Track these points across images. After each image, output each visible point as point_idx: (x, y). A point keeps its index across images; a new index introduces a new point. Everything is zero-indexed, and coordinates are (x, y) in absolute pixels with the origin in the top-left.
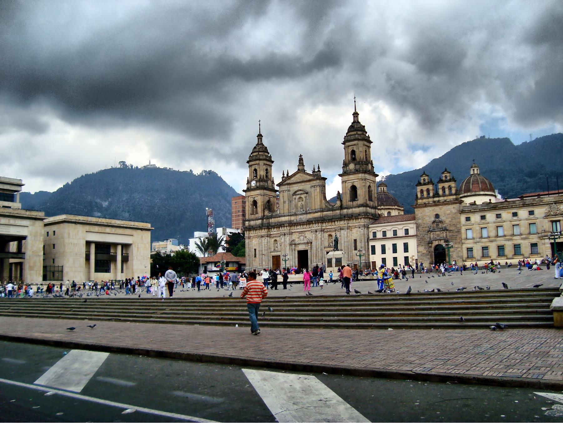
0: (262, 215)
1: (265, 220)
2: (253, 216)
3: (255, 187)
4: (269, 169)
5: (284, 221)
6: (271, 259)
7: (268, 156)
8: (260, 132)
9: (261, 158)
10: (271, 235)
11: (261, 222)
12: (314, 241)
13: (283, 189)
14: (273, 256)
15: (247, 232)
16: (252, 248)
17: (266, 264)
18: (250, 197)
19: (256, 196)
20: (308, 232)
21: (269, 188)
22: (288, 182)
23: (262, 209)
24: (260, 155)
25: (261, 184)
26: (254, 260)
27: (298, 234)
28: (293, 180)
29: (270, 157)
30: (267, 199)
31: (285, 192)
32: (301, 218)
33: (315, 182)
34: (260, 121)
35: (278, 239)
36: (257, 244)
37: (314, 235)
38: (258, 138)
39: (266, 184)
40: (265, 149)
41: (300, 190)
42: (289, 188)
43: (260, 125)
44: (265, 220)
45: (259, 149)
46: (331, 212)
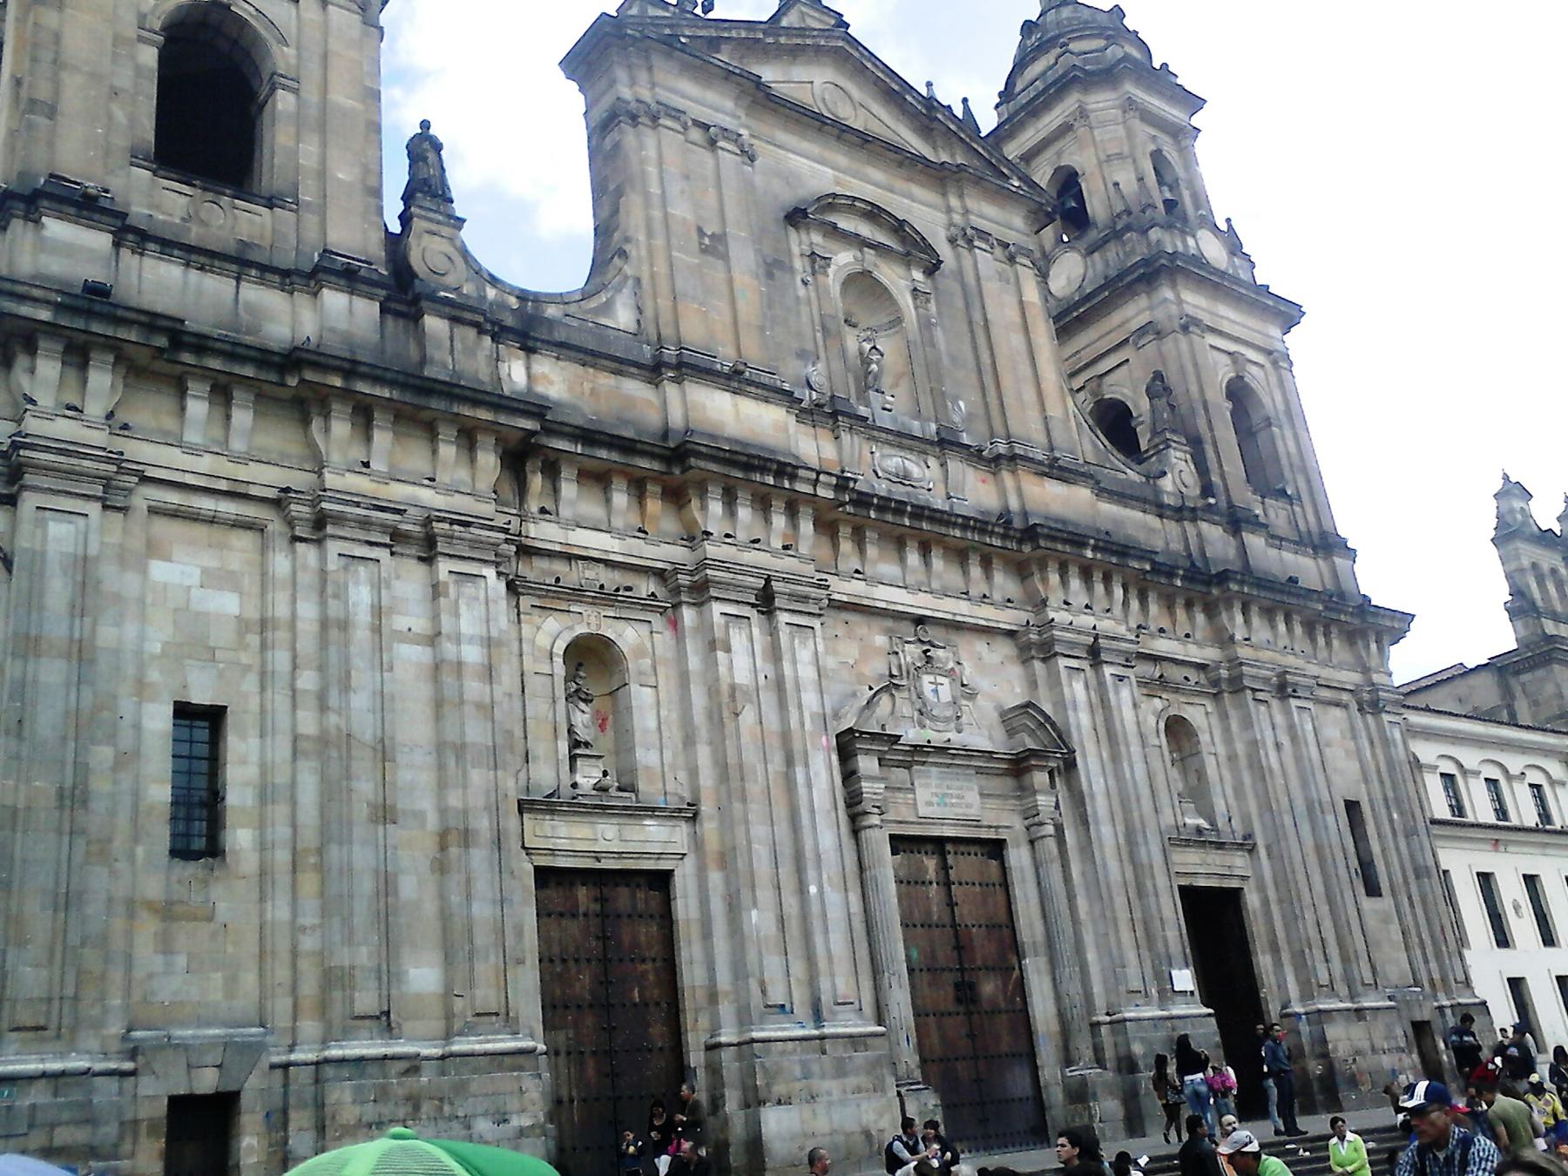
1: (434, 324)
6: (527, 915)
10: (526, 551)
12: (1090, 747)
14: (544, 876)
15: (102, 380)
16: (141, 687)
17: (486, 995)
20: (980, 645)
26: (168, 912)
27: (881, 640)
32: (904, 478)
33: (990, 210)
35: (627, 636)
36: (242, 625)
37: (1079, 687)
41: (874, 213)
44: (434, 324)
46: (1153, 521)
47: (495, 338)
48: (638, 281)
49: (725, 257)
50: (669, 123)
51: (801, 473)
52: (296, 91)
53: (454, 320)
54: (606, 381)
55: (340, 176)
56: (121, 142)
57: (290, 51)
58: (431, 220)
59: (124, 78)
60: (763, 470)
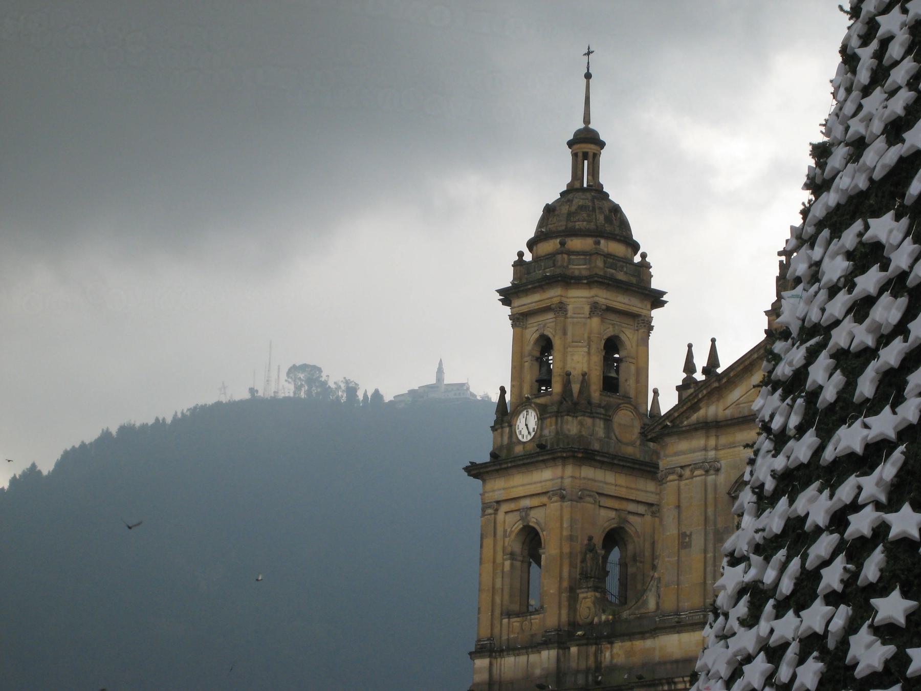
0: (564, 618)
1: (574, 650)
2: (516, 622)
3: (531, 448)
4: (629, 336)
5: (677, 662)
7: (631, 262)
8: (587, 120)
9: (579, 268)
11: (553, 665)
13: (683, 460)
18: (504, 507)
19: (535, 502)
21: (624, 459)
22: (711, 411)
23: (565, 584)
24: (570, 253)
25: (572, 426)
28: (737, 403)
29: (645, 266)
30: (605, 518)
31: (692, 477)
34: (589, 53)
38: (575, 155)
39: (600, 431)
40: (608, 219)
42: (712, 454)
43: (588, 76)
44: (574, 650)
45: (570, 215)
47: (596, 644)
48: (659, 579)
49: (690, 546)
50: (671, 477)
51: (676, 680)
52: (544, 553)
53: (577, 645)
54: (639, 644)
55: (551, 591)
56: (497, 612)
57: (544, 533)
58: (583, 593)
59: (498, 585)
60: (662, 684)
